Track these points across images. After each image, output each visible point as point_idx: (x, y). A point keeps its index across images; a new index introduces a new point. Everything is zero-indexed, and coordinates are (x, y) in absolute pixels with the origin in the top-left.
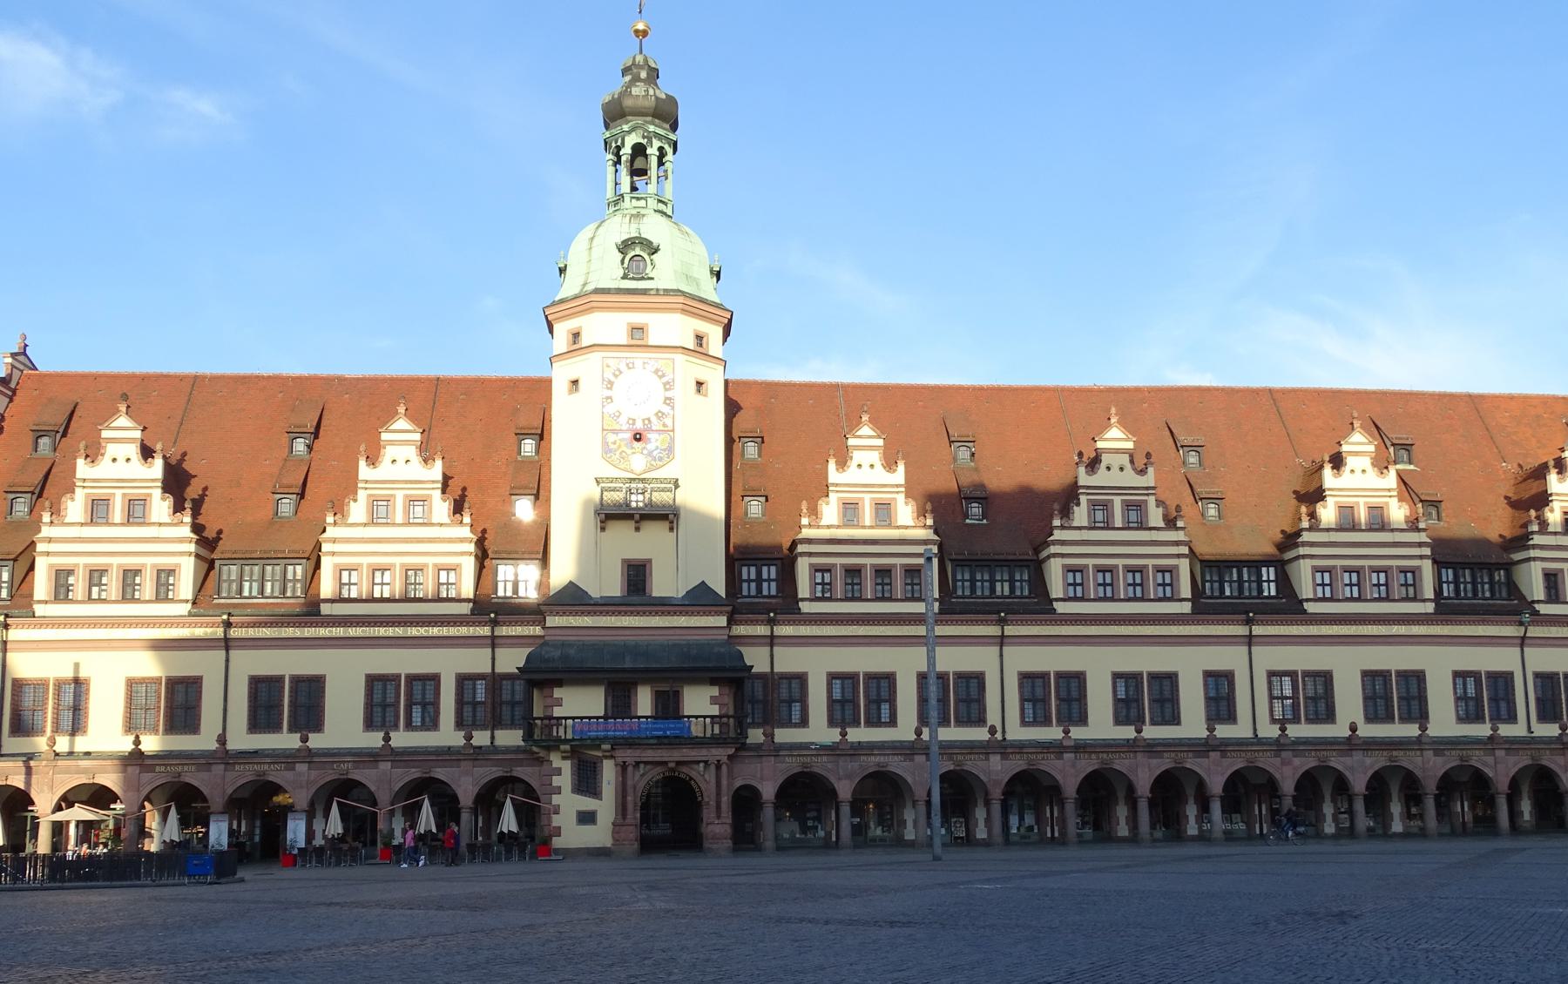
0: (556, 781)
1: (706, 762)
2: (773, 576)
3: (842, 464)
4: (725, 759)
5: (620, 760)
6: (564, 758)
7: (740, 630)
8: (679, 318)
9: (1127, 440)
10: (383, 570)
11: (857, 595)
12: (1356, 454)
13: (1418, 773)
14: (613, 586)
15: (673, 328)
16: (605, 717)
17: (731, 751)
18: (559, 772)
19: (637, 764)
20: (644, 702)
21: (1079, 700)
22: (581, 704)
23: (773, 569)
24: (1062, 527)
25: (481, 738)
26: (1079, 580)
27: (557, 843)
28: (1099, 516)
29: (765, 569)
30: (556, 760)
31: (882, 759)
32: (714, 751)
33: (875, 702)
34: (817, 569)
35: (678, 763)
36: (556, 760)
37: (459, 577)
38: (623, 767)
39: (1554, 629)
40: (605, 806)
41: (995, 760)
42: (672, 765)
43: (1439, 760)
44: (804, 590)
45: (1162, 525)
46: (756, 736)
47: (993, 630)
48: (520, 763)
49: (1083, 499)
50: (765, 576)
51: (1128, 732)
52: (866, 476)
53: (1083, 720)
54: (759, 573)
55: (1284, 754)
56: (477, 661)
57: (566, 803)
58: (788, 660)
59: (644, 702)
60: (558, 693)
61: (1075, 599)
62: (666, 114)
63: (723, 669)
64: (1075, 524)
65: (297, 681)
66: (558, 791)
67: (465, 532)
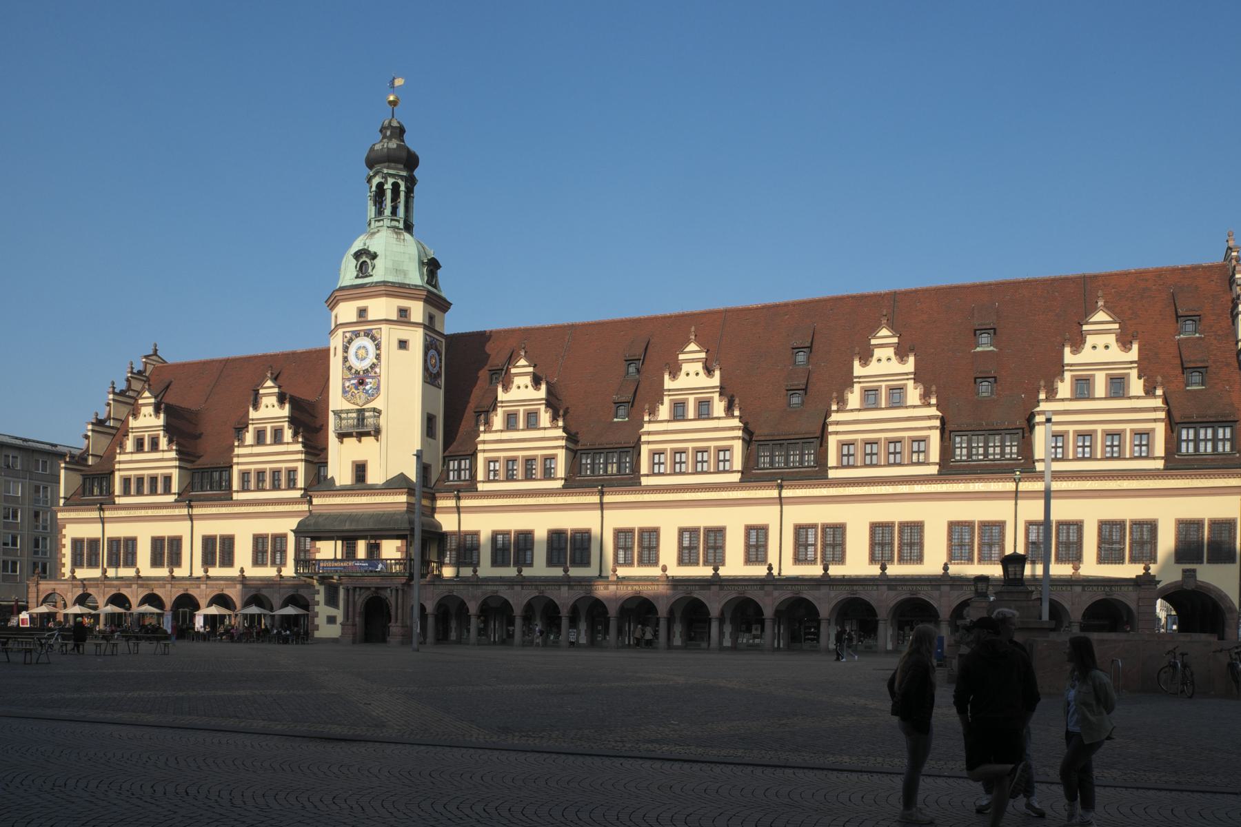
0: (317, 598)
3: (506, 388)
8: (384, 300)
12: (881, 346)
13: (873, 603)
15: (381, 308)
18: (318, 592)
19: (355, 588)
20: (361, 549)
21: (1150, 543)
22: (327, 550)
24: (650, 422)
26: (922, 449)
27: (317, 634)
31: (495, 588)
33: (692, 548)
35: (377, 588)
38: (347, 590)
39: (1172, 482)
40: (339, 613)
41: (564, 589)
43: (892, 593)
47: (1010, 486)
51: (558, 572)
53: (841, 560)
55: (767, 588)
57: (322, 610)
59: (361, 549)
62: (411, 162)
63: (394, 530)
66: (318, 603)
67: (299, 447)
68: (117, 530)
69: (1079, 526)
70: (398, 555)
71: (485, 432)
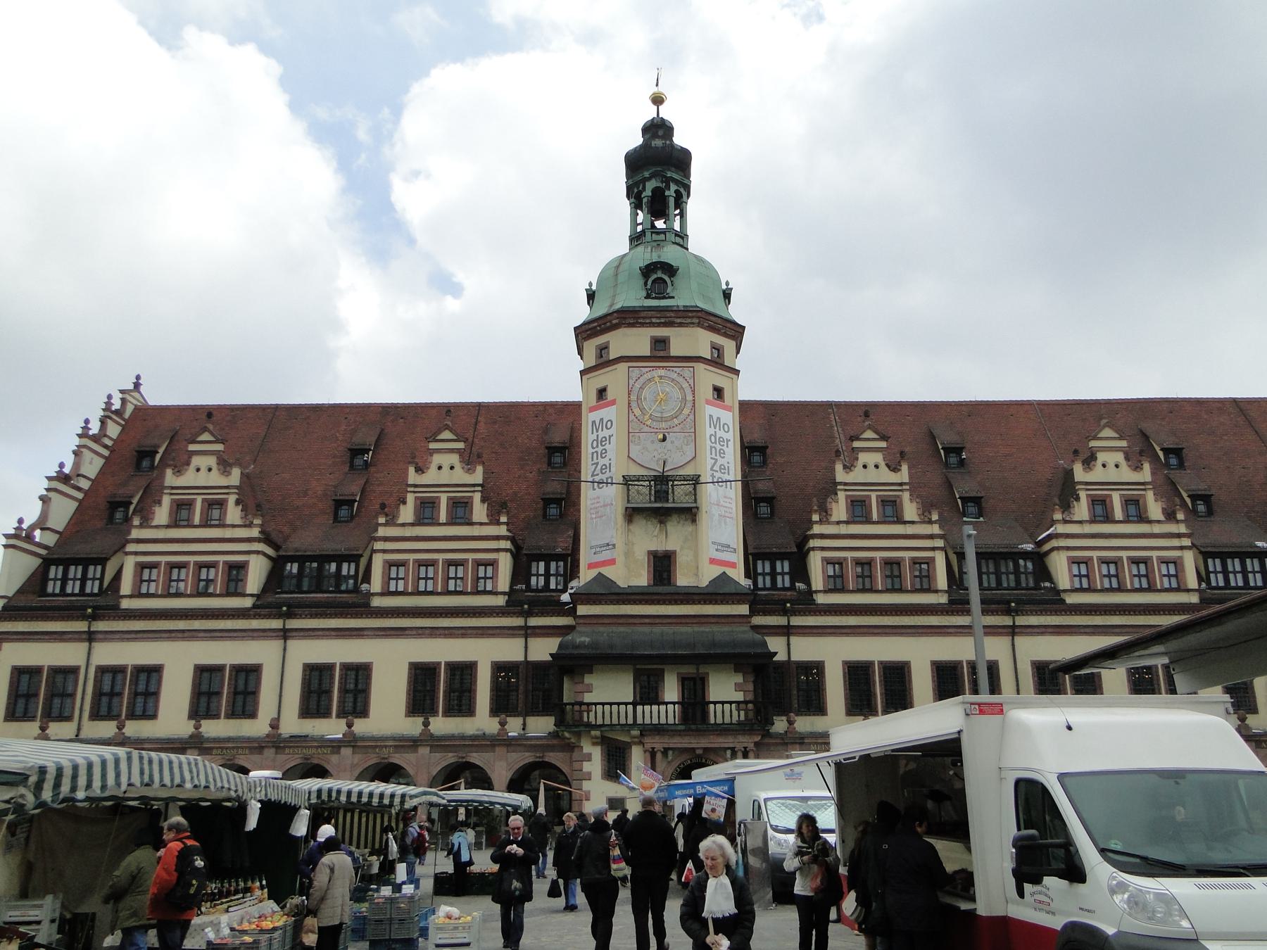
0: (587, 767)
1: (733, 749)
2: (787, 569)
4: (751, 746)
5: (648, 746)
6: (594, 744)
7: (758, 620)
9: (1121, 438)
10: (427, 566)
11: (868, 586)
14: (642, 579)
16: (635, 704)
17: (757, 739)
18: (588, 758)
20: (671, 691)
23: (786, 564)
25: (514, 726)
28: (1099, 509)
29: (778, 564)
30: (587, 747)
32: (741, 738)
34: (828, 562)
35: (705, 749)
36: (587, 747)
37: (496, 571)
42: (699, 752)
44: (817, 582)
45: (1162, 518)
46: (780, 725)
48: (551, 748)
49: (1083, 495)
50: (779, 570)
52: (872, 476)
54: (773, 568)
56: (510, 650)
58: (804, 649)
59: (671, 691)
60: (588, 679)
61: (1081, 590)
64: (1076, 518)
65: (347, 667)
67: (503, 530)
68: (109, 654)
69: (1156, 666)
70: (739, 696)
71: (821, 522)
